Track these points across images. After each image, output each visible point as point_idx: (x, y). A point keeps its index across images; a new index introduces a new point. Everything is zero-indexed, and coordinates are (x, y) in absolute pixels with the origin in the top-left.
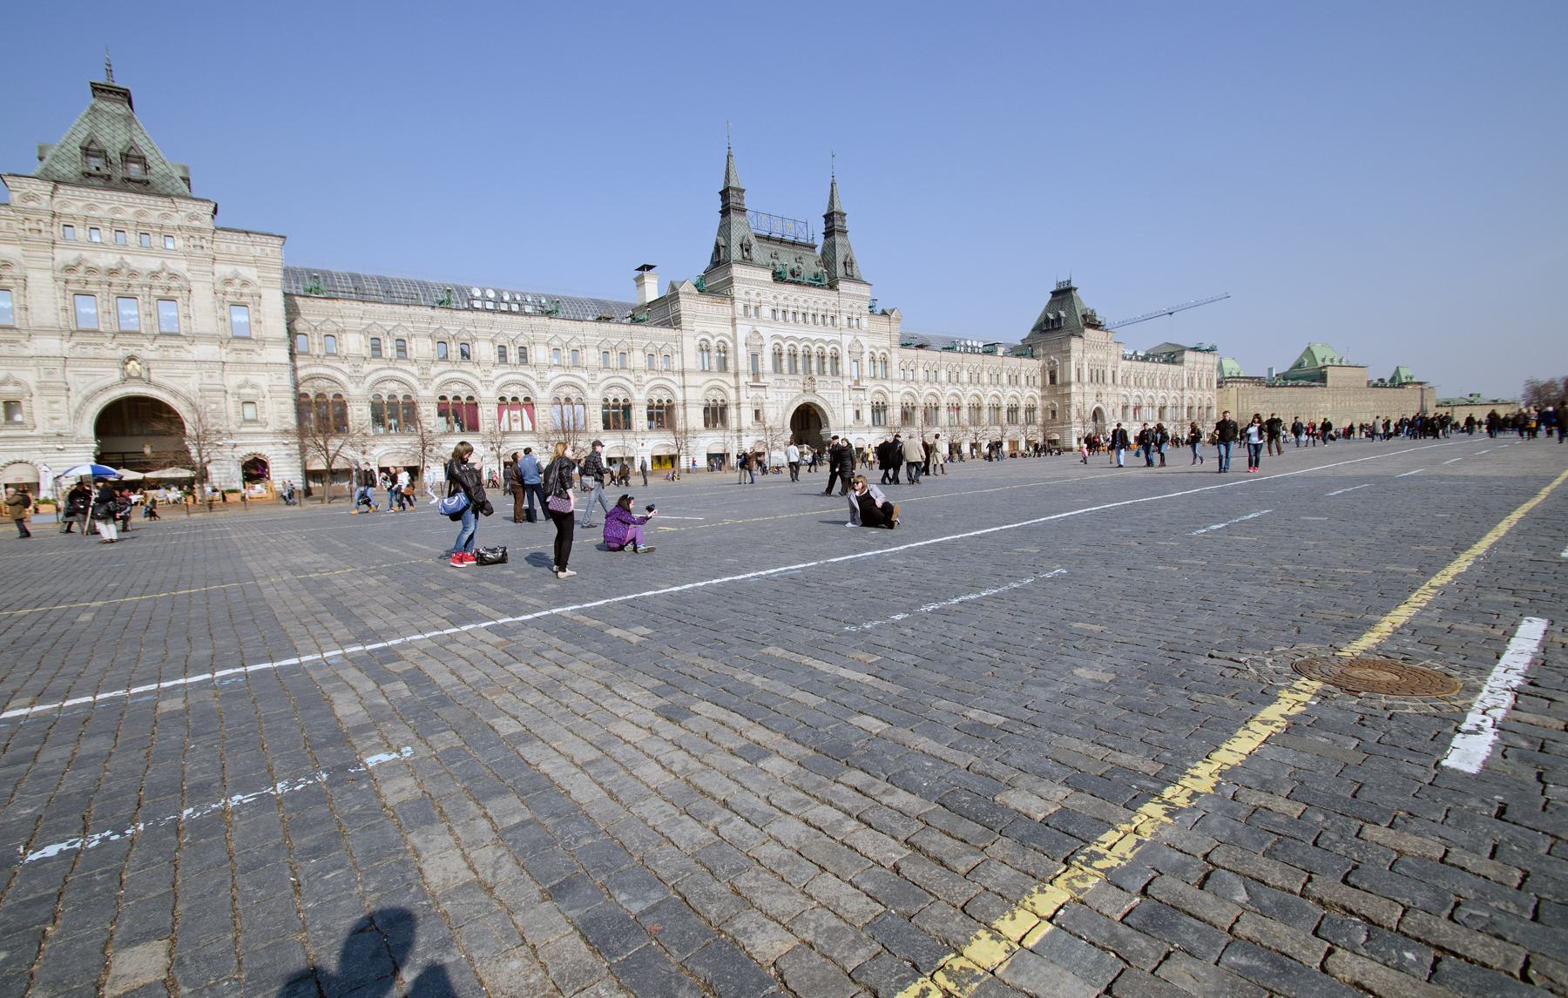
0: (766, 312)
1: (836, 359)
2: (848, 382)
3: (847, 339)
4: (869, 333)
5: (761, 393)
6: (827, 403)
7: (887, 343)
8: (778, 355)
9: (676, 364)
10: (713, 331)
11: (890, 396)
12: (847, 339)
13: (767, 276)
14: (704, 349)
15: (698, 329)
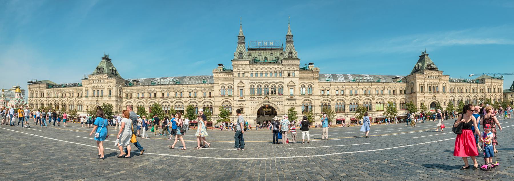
0: (246, 74)
1: (281, 88)
2: (286, 97)
3: (286, 81)
4: (299, 78)
5: (243, 103)
6: (276, 106)
7: (312, 81)
8: (252, 89)
9: (212, 95)
10: (226, 83)
11: (313, 102)
12: (286, 81)
13: (248, 63)
14: (223, 88)
15: (220, 83)
